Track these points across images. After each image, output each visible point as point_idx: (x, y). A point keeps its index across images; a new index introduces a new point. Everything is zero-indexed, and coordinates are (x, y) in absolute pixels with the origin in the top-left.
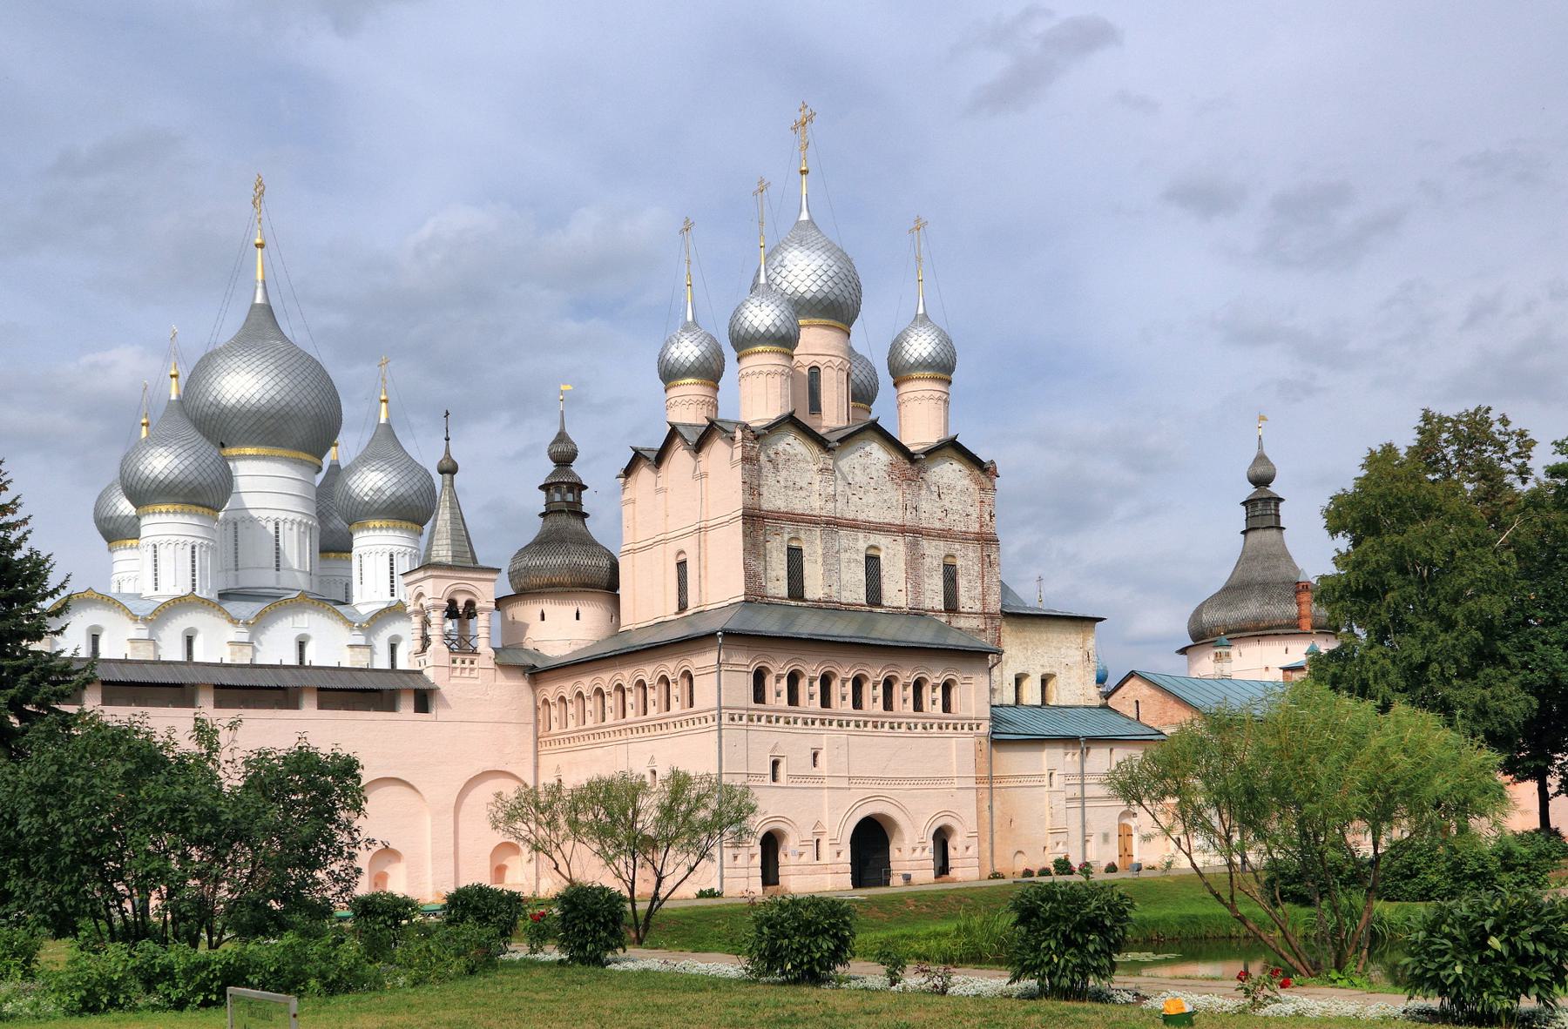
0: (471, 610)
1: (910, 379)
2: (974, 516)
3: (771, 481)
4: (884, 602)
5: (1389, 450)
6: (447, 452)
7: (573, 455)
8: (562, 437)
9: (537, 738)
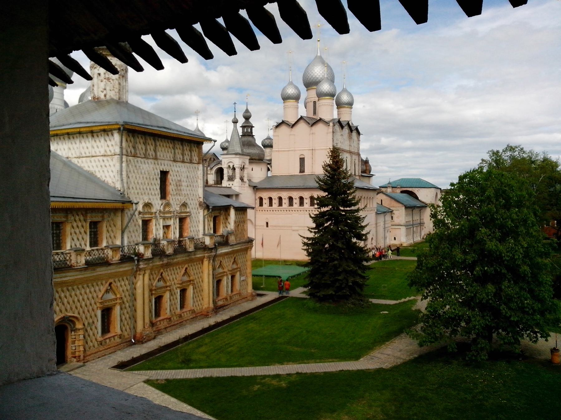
1: (344, 107)
5: (557, 166)
7: (250, 117)
8: (247, 111)
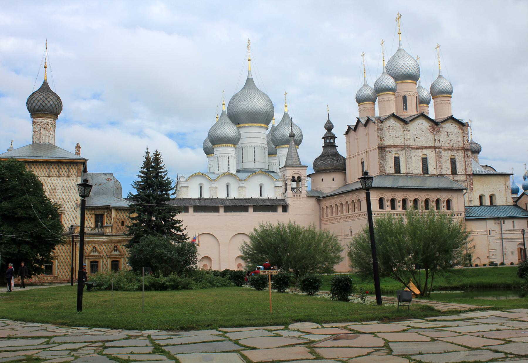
0: (299, 179)
2: (462, 141)
3: (388, 135)
4: (430, 173)
6: (292, 131)
8: (329, 122)
9: (321, 219)
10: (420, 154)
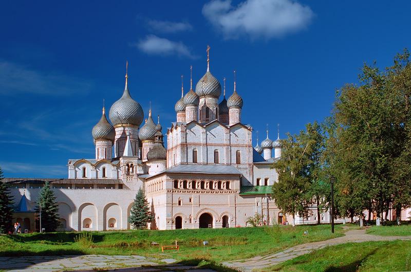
10: (213, 148)
